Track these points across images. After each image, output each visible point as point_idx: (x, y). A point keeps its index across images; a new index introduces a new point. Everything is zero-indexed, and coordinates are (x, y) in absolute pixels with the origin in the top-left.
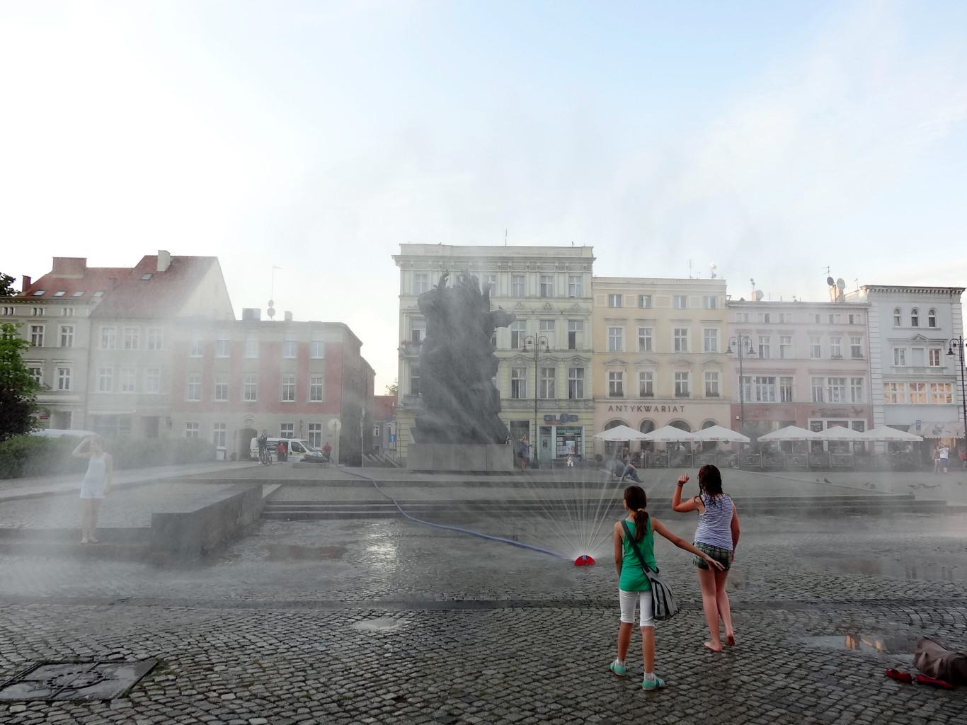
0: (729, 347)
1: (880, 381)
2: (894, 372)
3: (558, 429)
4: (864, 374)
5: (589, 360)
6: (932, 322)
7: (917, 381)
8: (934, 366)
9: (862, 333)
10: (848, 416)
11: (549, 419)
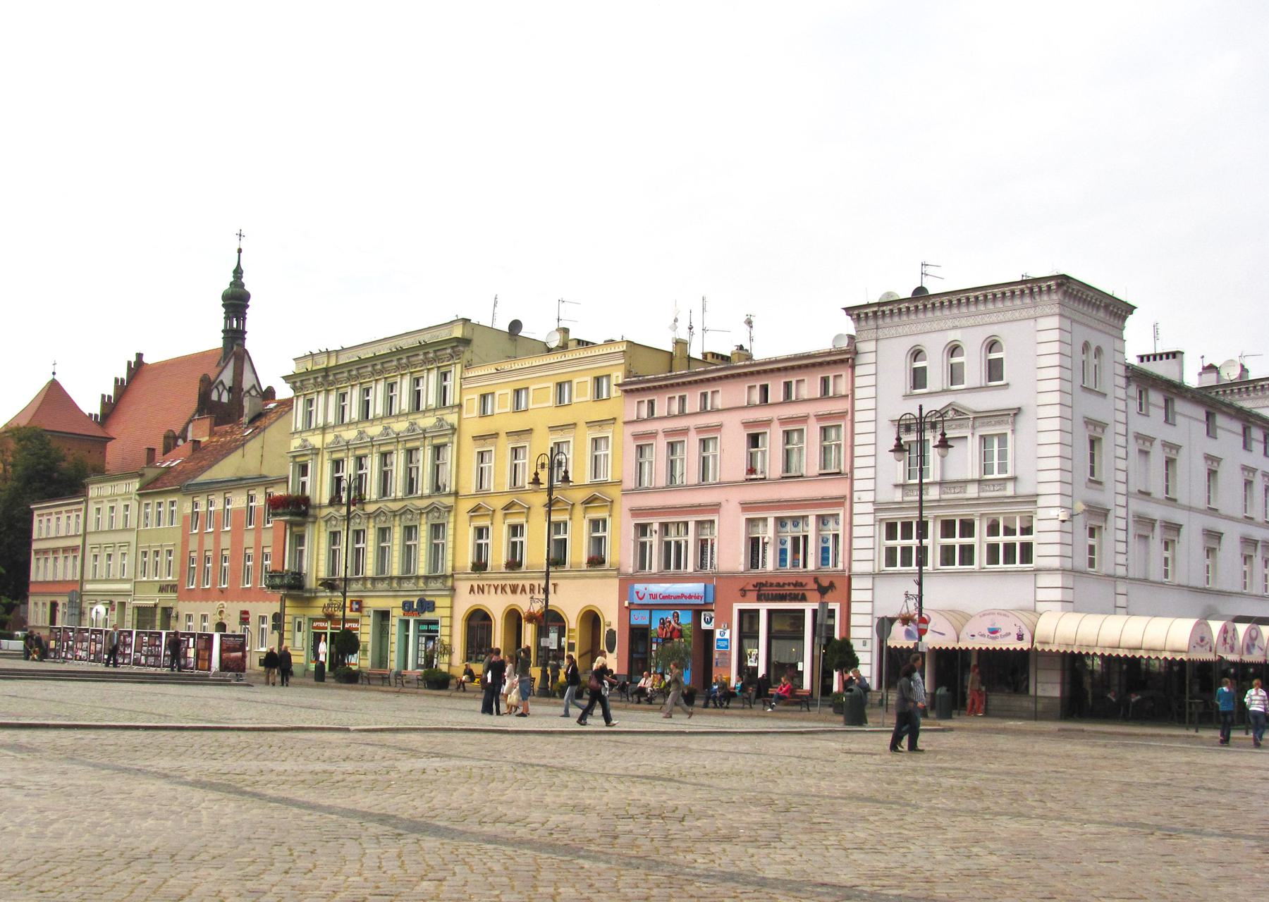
0: (536, 474)
1: (870, 519)
2: (898, 495)
3: (419, 623)
4: (841, 504)
5: (449, 509)
6: (995, 370)
7: (957, 514)
8: (996, 475)
9: (842, 415)
10: (803, 599)
11: (407, 607)
